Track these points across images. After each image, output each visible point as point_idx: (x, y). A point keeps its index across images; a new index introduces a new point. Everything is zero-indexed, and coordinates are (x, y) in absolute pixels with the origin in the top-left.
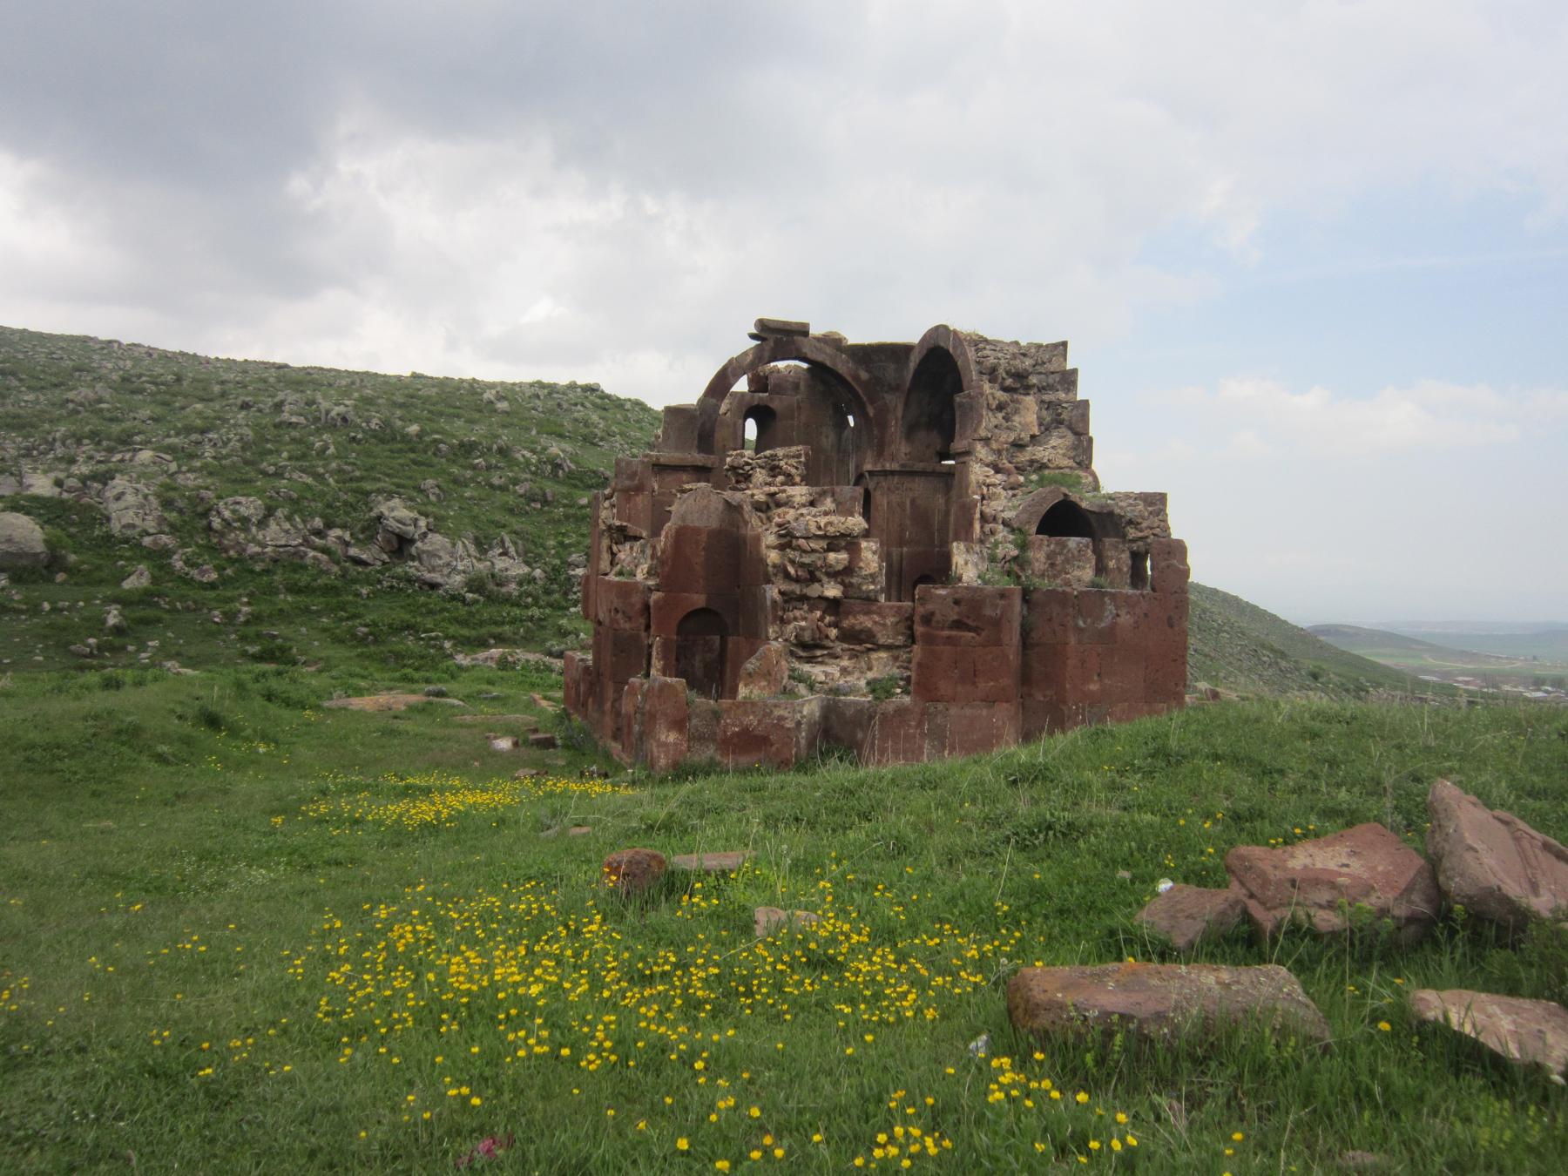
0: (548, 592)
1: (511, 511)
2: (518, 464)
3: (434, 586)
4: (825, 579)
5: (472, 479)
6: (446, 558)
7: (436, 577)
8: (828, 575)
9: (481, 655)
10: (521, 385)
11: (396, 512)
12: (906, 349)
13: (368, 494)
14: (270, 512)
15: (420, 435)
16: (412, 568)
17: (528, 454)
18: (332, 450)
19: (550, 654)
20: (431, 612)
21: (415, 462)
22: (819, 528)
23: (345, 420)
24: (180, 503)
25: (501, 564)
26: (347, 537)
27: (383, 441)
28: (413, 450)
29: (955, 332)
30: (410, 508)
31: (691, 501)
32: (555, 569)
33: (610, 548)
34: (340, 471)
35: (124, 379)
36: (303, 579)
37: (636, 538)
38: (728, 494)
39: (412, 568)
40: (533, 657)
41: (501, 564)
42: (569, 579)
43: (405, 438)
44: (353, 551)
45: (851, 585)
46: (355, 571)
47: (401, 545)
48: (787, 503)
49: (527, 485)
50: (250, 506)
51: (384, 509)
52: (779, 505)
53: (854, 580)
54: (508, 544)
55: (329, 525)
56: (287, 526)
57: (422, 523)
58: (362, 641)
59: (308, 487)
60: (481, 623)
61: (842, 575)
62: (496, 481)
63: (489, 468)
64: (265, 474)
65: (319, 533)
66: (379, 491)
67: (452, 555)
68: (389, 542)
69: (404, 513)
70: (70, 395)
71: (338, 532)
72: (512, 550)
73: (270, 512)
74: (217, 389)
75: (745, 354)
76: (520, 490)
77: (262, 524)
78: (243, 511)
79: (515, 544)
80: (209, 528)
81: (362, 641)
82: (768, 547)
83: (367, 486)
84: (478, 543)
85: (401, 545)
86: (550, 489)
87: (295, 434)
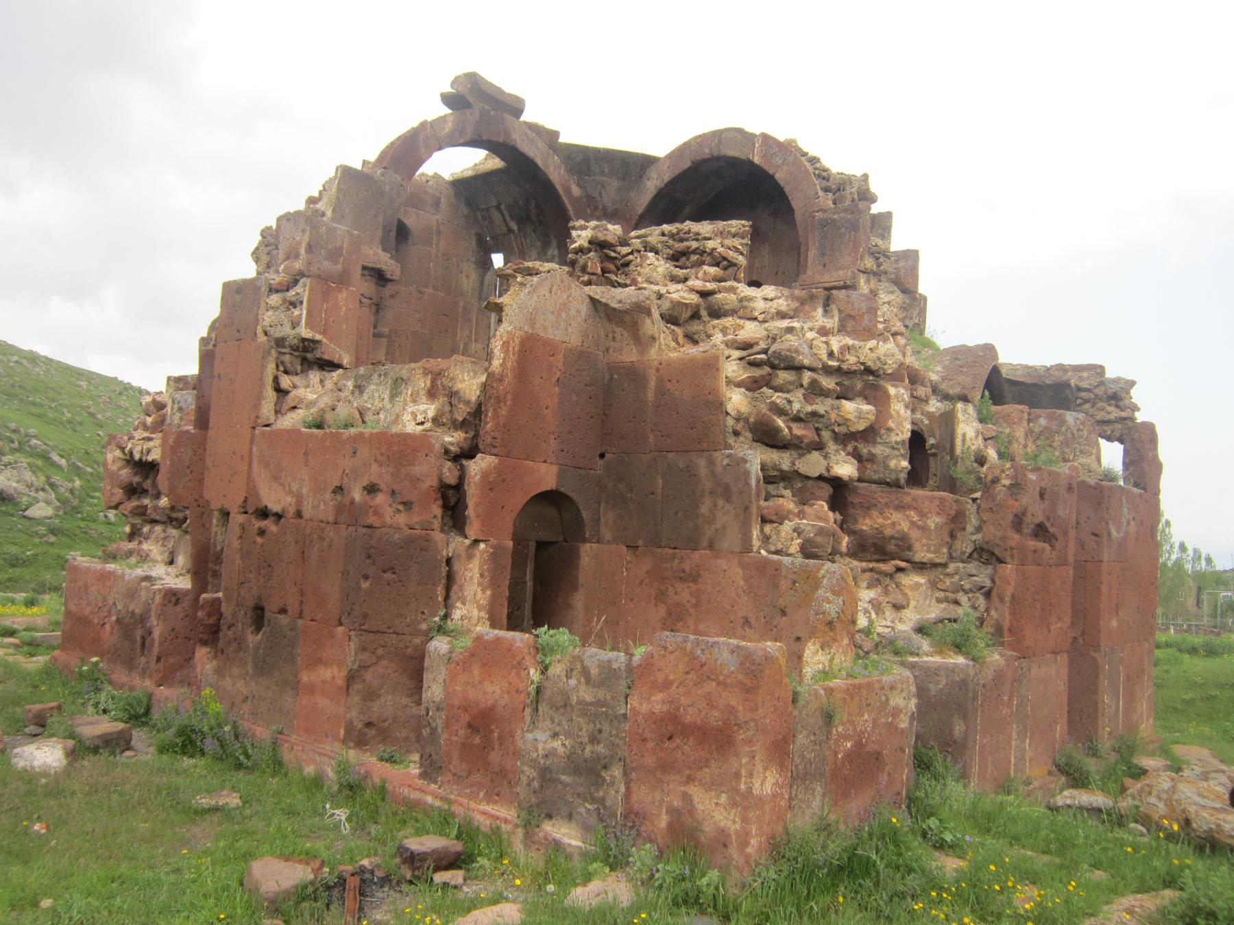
4: (832, 447)
8: (837, 437)
12: (646, 162)
22: (831, 354)
29: (766, 138)
31: (544, 290)
33: (276, 379)
37: (328, 365)
38: (597, 291)
45: (872, 458)
48: (742, 311)
52: (716, 313)
53: (878, 450)
61: (856, 440)
75: (442, 119)
82: (729, 382)
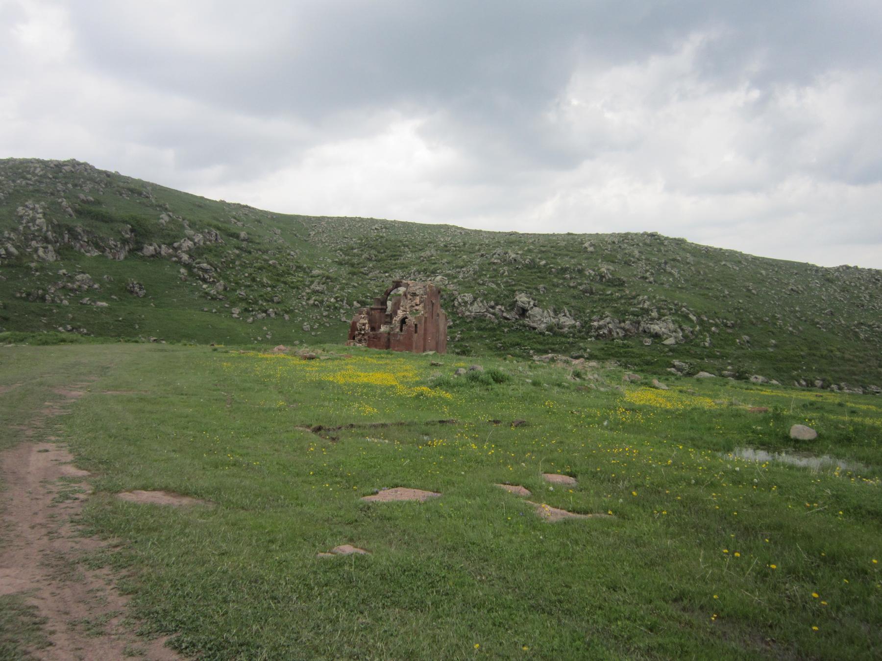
0: (580, 332)
1: (574, 297)
2: (585, 276)
3: (534, 328)
5: (562, 284)
6: (539, 317)
7: (535, 325)
9: (544, 356)
10: (607, 235)
11: (522, 299)
13: (514, 291)
14: (475, 299)
15: (545, 266)
16: (526, 321)
17: (591, 272)
18: (506, 273)
19: (572, 357)
20: (529, 339)
21: (539, 277)
23: (515, 260)
24: (445, 297)
25: (563, 319)
26: (503, 309)
27: (530, 268)
28: (540, 272)
30: (528, 297)
32: (586, 322)
34: (507, 282)
35: (446, 246)
36: (483, 325)
39: (526, 321)
40: (564, 358)
41: (563, 319)
42: (591, 326)
43: (539, 267)
44: (505, 314)
46: (503, 321)
47: (523, 312)
49: (584, 286)
50: (468, 297)
51: (517, 298)
54: (566, 311)
55: (497, 304)
56: (481, 304)
57: (532, 303)
58: (499, 349)
59: (493, 289)
60: (548, 344)
62: (572, 284)
63: (571, 278)
64: (479, 284)
65: (493, 307)
66: (519, 290)
67: (542, 316)
68: (518, 310)
69: (525, 299)
70: (422, 254)
71: (499, 307)
72: (568, 314)
73: (475, 299)
74: (477, 248)
76: (581, 288)
77: (472, 304)
78: (466, 299)
79: (570, 311)
80: (454, 306)
81: (499, 349)
83: (515, 288)
84: (555, 311)
85: (523, 312)
86: (596, 287)
87: (495, 267)
